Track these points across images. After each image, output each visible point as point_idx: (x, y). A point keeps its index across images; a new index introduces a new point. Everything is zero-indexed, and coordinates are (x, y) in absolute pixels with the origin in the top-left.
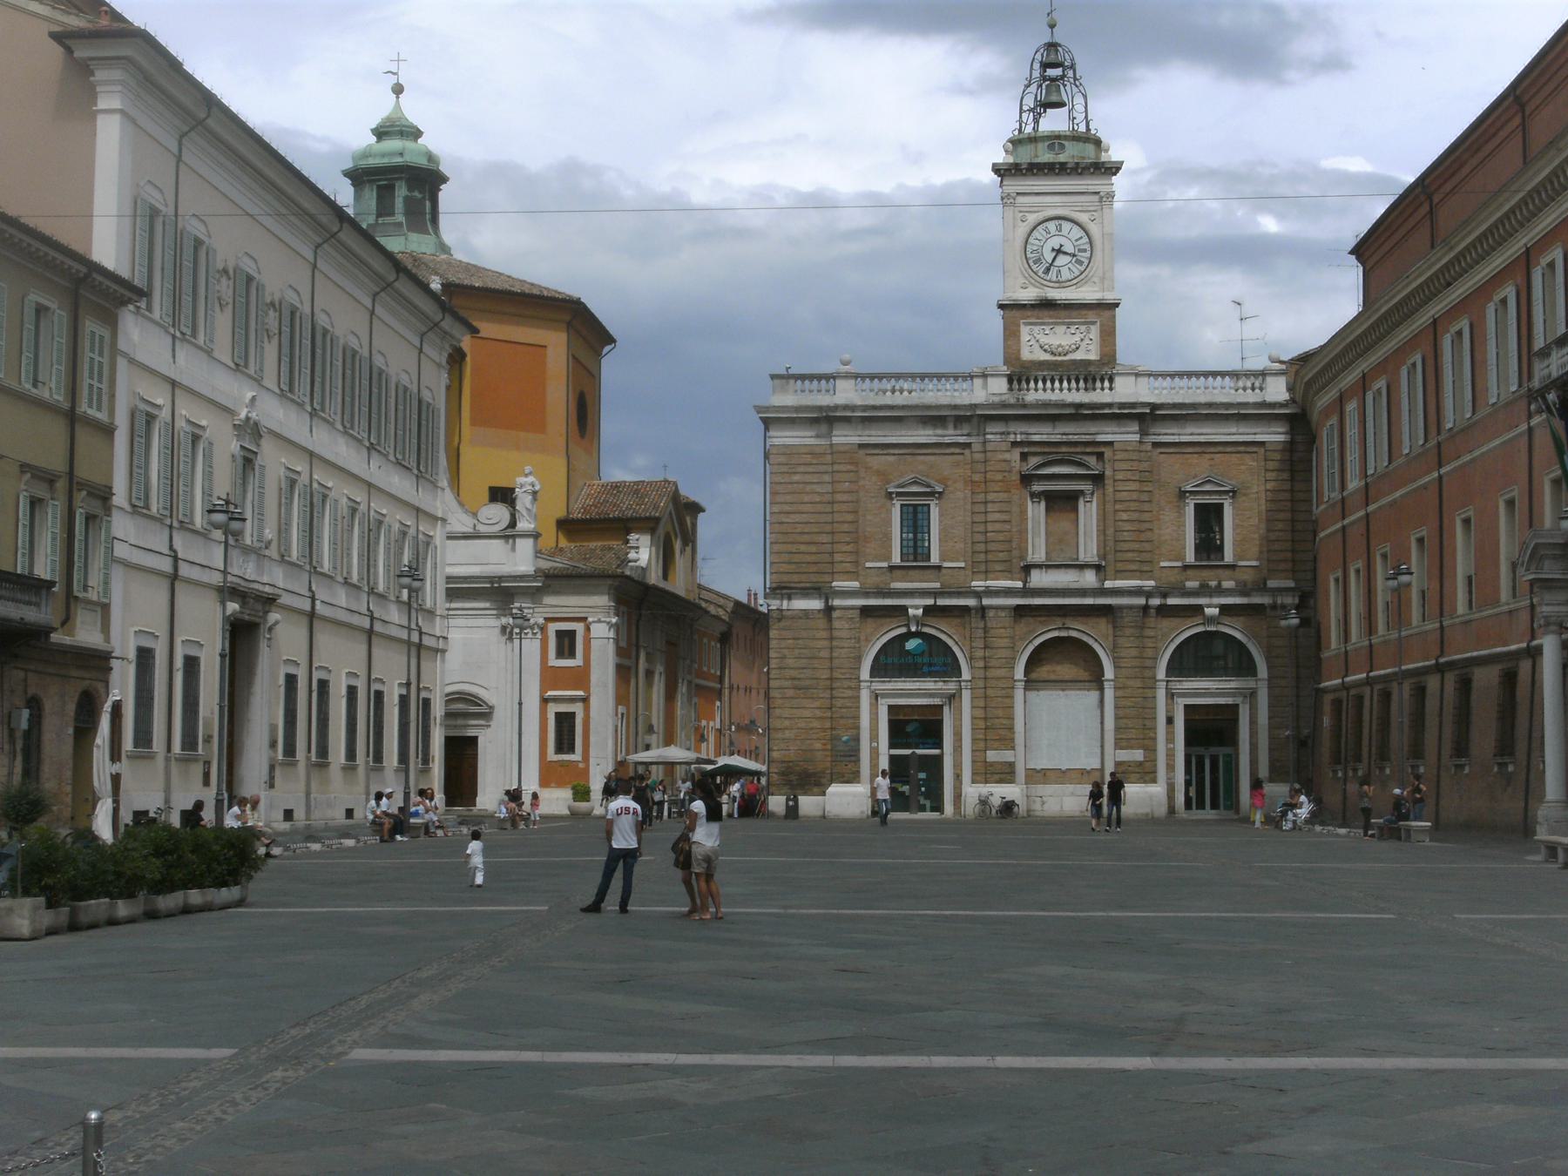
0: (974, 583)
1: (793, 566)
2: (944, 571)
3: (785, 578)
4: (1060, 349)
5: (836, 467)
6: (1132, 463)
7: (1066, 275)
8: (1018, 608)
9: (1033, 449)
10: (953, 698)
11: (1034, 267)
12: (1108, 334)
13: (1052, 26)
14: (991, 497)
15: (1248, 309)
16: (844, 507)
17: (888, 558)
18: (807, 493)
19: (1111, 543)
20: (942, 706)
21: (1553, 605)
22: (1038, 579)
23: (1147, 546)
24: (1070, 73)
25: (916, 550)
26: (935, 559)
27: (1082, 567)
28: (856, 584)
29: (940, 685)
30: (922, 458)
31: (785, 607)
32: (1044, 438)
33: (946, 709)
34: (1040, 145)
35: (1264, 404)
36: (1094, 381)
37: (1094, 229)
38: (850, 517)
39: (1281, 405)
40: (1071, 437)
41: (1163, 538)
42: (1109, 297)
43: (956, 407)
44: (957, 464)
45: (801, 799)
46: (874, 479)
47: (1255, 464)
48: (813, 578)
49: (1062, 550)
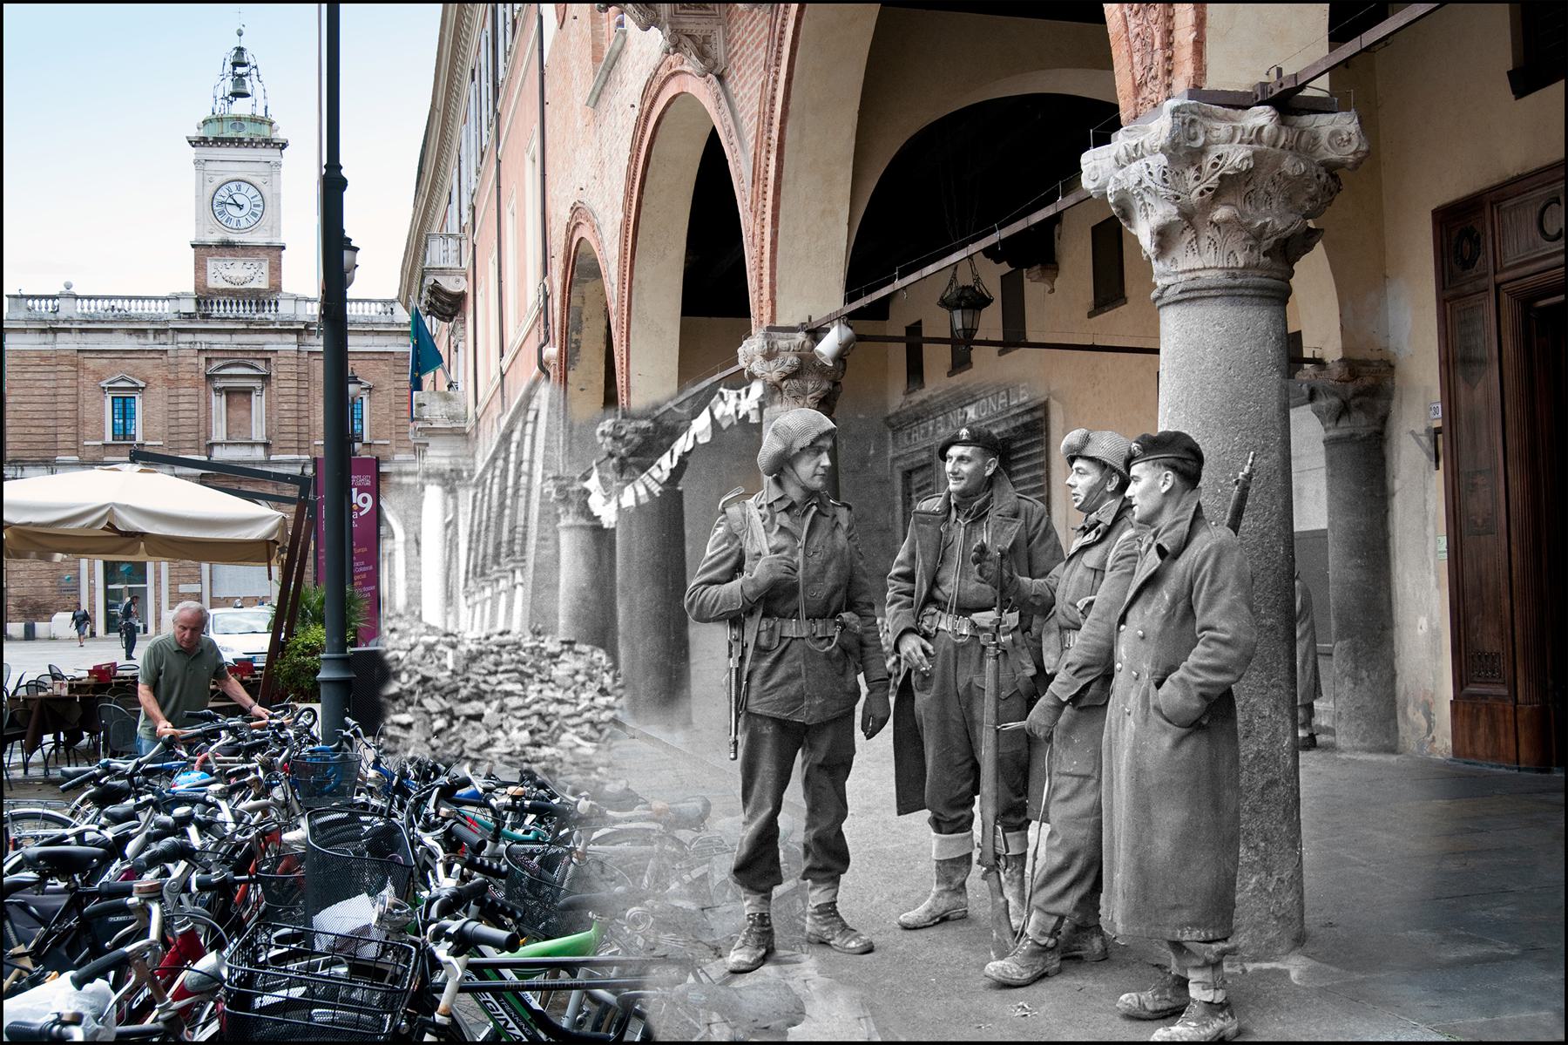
3: (19, 453)
5: (59, 368)
7: (244, 224)
9: (215, 355)
12: (276, 269)
13: (240, 35)
14: (182, 391)
16: (67, 399)
17: (104, 438)
23: (304, 429)
24: (254, 71)
27: (253, 445)
28: (76, 458)
32: (224, 347)
36: (264, 303)
37: (265, 189)
38: (70, 407)
39: (405, 325)
42: (276, 242)
44: (157, 366)
45: (37, 624)
46: (91, 377)
48: (42, 454)
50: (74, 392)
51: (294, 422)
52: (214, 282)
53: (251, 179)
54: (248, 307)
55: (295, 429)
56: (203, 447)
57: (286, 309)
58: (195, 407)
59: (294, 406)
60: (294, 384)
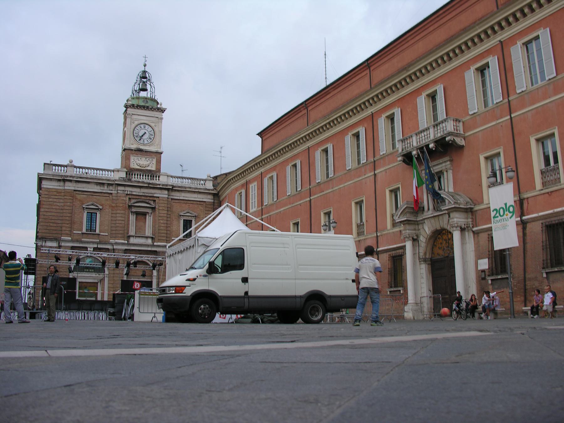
0: (111, 241)
1: (47, 231)
2: (100, 236)
3: (44, 235)
4: (143, 166)
5: (66, 197)
7: (146, 142)
8: (126, 250)
9: (133, 197)
10: (102, 280)
11: (136, 138)
12: (159, 162)
14: (118, 212)
15: (184, 168)
17: (82, 230)
18: (54, 205)
19: (157, 230)
20: (97, 283)
22: (132, 240)
23: (168, 232)
25: (91, 228)
27: (147, 237)
28: (70, 238)
29: (97, 275)
30: (94, 196)
31: (43, 245)
32: (137, 194)
33: (99, 284)
34: (140, 100)
35: (206, 189)
36: (154, 176)
37: (156, 129)
38: (69, 215)
39: (212, 190)
40: (145, 194)
41: (173, 230)
42: (160, 151)
43: (108, 180)
44: (107, 200)
46: (78, 202)
47: (202, 208)
48: (54, 235)
49: (140, 232)
50: (71, 208)
51: (165, 228)
52: (134, 165)
54: (147, 177)
55: (165, 232)
56: (126, 237)
57: (163, 180)
58: (123, 219)
59: (165, 222)
60: (166, 212)
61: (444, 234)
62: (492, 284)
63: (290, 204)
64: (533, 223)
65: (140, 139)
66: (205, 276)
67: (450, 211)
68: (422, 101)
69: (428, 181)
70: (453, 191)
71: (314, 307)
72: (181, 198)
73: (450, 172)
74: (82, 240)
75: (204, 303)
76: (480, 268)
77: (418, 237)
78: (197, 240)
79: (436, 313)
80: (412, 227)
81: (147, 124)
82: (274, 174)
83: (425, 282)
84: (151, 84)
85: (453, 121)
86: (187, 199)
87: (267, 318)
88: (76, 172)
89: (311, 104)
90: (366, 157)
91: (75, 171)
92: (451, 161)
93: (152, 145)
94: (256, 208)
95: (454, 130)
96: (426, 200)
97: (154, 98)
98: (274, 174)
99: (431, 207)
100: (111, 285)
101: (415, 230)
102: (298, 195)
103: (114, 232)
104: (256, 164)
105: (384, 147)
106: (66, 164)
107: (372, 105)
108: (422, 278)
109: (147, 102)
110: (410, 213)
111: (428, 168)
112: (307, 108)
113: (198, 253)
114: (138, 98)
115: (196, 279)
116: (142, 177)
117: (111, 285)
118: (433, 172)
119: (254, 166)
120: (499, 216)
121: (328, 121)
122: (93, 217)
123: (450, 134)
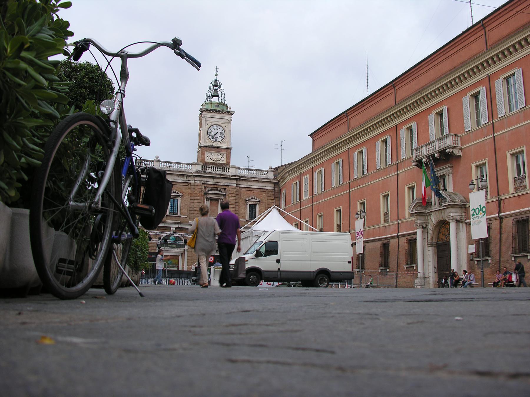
2: (181, 218)
6: (234, 192)
7: (218, 140)
9: (208, 186)
10: (183, 254)
12: (229, 157)
13: (216, 76)
14: (196, 198)
20: (179, 256)
21: (421, 220)
26: (179, 214)
30: (176, 186)
32: (211, 183)
33: (180, 257)
35: (268, 179)
36: (224, 169)
37: (226, 129)
39: (273, 179)
40: (218, 183)
41: (241, 213)
42: (229, 147)
44: (186, 189)
52: (208, 160)
53: (221, 124)
54: (219, 169)
57: (232, 172)
60: (234, 198)
61: (446, 224)
62: (477, 264)
63: (334, 194)
64: (507, 219)
65: (213, 138)
66: (254, 258)
67: (448, 207)
68: (432, 118)
69: (432, 183)
70: (453, 191)
71: (322, 278)
72: (247, 186)
73: (451, 176)
74: (167, 221)
75: (253, 275)
76: (470, 251)
77: (427, 226)
78: (252, 232)
79: (440, 284)
80: (422, 218)
81: (218, 125)
82: (322, 169)
83: (431, 261)
84: (222, 90)
85: (453, 136)
86: (252, 187)
87: (298, 285)
88: (162, 166)
89: (350, 113)
90: (391, 159)
91: (160, 165)
92: (452, 167)
93: (223, 142)
94: (308, 196)
95: (453, 144)
96: (433, 198)
97: (224, 103)
98: (322, 169)
99: (437, 202)
100: (189, 258)
101: (424, 220)
102: (340, 187)
103: (192, 215)
104: (308, 160)
105: (404, 153)
106: (153, 159)
107: (396, 119)
108: (430, 257)
109: (219, 106)
110: (421, 207)
111: (433, 173)
112: (347, 117)
113: (253, 241)
114: (211, 103)
115: (248, 260)
116: (214, 169)
117: (189, 258)
118: (437, 175)
119: (306, 161)
120: (476, 215)
121: (363, 129)
122: (175, 202)
123: (449, 147)
